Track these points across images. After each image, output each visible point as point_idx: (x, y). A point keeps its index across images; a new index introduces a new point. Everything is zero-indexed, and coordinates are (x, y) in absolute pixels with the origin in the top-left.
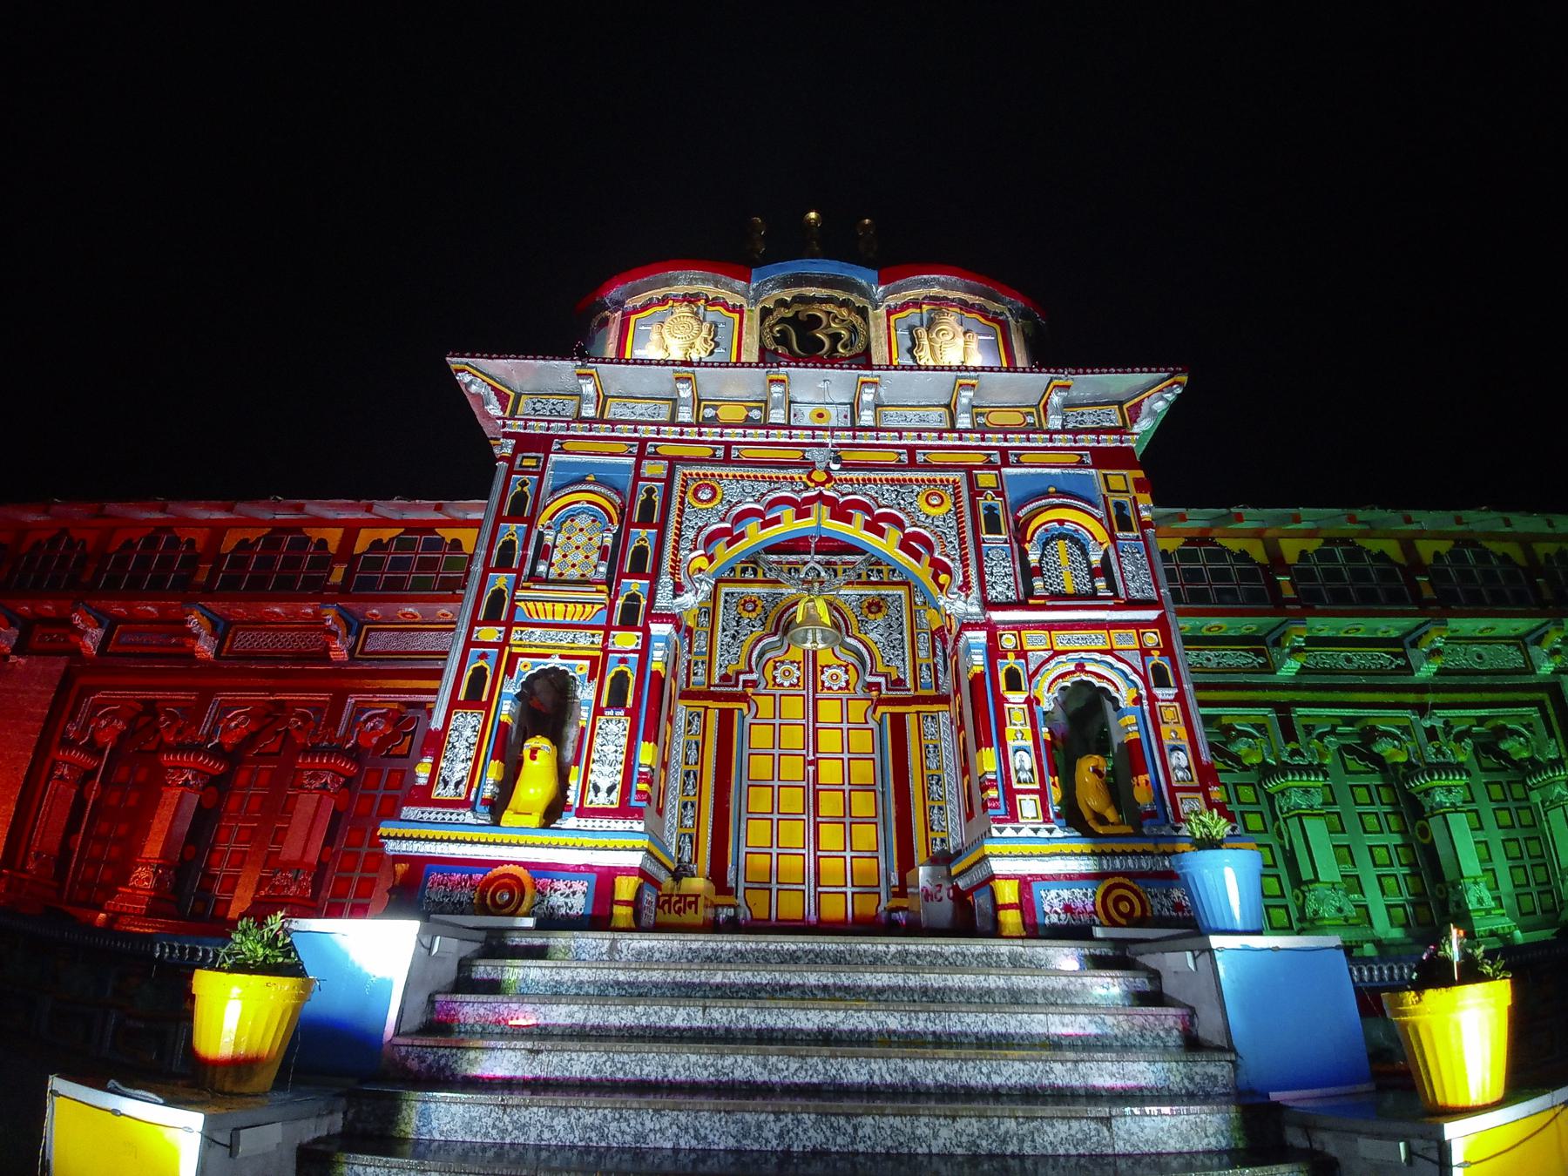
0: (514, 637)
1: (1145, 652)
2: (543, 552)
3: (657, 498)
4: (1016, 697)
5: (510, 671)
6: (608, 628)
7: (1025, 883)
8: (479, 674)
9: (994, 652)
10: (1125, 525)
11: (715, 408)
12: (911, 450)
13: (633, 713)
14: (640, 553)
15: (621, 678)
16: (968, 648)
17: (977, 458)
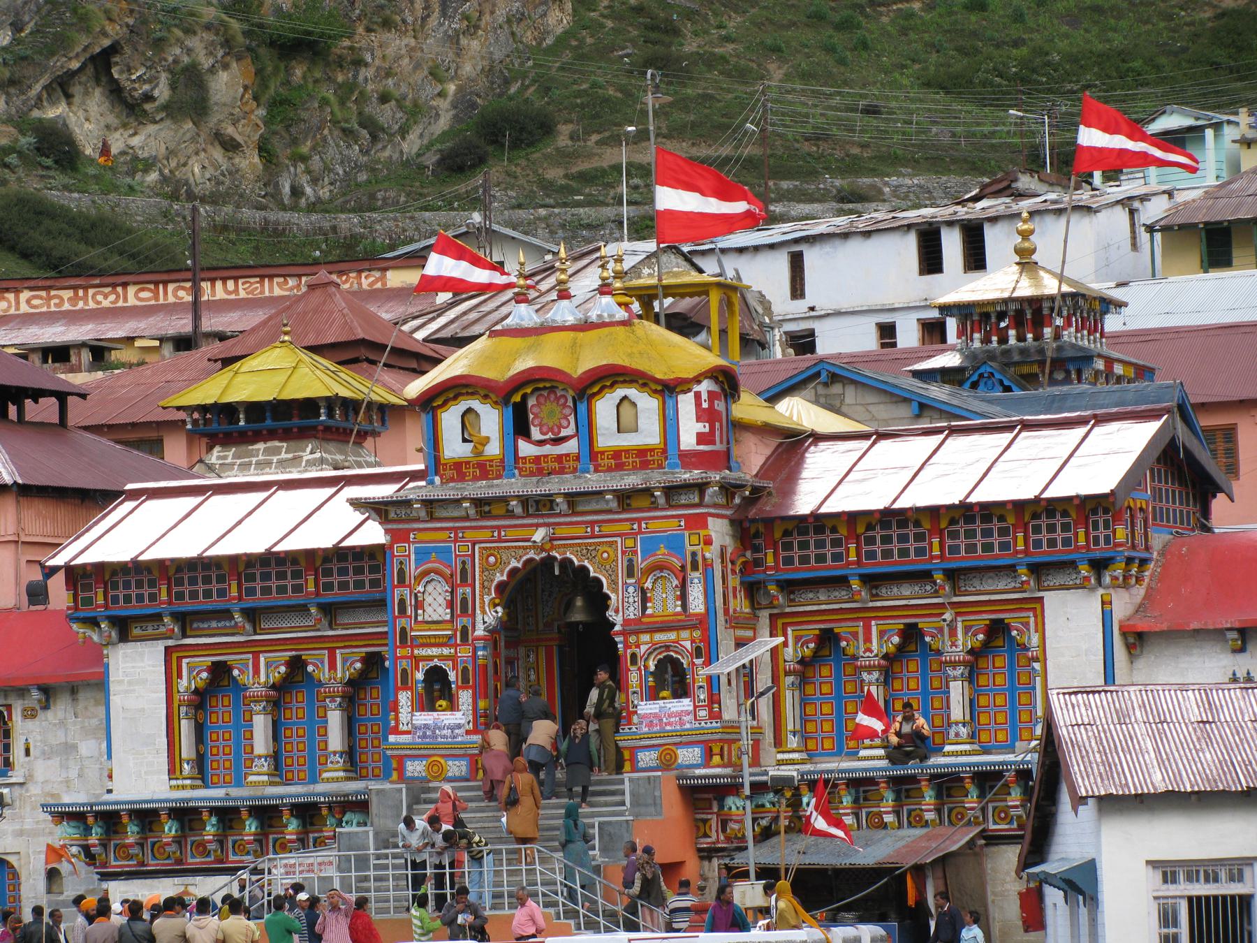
0: (416, 652)
1: (693, 642)
2: (419, 605)
3: (468, 567)
4: (632, 668)
5: (417, 668)
6: (456, 646)
7: (634, 750)
8: (404, 671)
9: (627, 646)
10: (695, 567)
11: (489, 504)
12: (593, 523)
13: (474, 688)
14: (464, 600)
15: (465, 670)
16: (616, 644)
17: (624, 528)
